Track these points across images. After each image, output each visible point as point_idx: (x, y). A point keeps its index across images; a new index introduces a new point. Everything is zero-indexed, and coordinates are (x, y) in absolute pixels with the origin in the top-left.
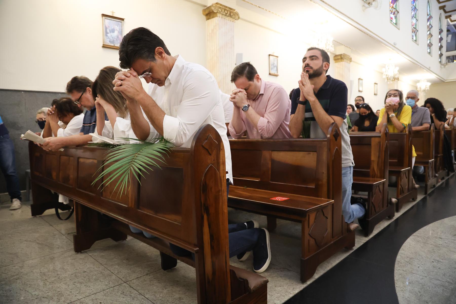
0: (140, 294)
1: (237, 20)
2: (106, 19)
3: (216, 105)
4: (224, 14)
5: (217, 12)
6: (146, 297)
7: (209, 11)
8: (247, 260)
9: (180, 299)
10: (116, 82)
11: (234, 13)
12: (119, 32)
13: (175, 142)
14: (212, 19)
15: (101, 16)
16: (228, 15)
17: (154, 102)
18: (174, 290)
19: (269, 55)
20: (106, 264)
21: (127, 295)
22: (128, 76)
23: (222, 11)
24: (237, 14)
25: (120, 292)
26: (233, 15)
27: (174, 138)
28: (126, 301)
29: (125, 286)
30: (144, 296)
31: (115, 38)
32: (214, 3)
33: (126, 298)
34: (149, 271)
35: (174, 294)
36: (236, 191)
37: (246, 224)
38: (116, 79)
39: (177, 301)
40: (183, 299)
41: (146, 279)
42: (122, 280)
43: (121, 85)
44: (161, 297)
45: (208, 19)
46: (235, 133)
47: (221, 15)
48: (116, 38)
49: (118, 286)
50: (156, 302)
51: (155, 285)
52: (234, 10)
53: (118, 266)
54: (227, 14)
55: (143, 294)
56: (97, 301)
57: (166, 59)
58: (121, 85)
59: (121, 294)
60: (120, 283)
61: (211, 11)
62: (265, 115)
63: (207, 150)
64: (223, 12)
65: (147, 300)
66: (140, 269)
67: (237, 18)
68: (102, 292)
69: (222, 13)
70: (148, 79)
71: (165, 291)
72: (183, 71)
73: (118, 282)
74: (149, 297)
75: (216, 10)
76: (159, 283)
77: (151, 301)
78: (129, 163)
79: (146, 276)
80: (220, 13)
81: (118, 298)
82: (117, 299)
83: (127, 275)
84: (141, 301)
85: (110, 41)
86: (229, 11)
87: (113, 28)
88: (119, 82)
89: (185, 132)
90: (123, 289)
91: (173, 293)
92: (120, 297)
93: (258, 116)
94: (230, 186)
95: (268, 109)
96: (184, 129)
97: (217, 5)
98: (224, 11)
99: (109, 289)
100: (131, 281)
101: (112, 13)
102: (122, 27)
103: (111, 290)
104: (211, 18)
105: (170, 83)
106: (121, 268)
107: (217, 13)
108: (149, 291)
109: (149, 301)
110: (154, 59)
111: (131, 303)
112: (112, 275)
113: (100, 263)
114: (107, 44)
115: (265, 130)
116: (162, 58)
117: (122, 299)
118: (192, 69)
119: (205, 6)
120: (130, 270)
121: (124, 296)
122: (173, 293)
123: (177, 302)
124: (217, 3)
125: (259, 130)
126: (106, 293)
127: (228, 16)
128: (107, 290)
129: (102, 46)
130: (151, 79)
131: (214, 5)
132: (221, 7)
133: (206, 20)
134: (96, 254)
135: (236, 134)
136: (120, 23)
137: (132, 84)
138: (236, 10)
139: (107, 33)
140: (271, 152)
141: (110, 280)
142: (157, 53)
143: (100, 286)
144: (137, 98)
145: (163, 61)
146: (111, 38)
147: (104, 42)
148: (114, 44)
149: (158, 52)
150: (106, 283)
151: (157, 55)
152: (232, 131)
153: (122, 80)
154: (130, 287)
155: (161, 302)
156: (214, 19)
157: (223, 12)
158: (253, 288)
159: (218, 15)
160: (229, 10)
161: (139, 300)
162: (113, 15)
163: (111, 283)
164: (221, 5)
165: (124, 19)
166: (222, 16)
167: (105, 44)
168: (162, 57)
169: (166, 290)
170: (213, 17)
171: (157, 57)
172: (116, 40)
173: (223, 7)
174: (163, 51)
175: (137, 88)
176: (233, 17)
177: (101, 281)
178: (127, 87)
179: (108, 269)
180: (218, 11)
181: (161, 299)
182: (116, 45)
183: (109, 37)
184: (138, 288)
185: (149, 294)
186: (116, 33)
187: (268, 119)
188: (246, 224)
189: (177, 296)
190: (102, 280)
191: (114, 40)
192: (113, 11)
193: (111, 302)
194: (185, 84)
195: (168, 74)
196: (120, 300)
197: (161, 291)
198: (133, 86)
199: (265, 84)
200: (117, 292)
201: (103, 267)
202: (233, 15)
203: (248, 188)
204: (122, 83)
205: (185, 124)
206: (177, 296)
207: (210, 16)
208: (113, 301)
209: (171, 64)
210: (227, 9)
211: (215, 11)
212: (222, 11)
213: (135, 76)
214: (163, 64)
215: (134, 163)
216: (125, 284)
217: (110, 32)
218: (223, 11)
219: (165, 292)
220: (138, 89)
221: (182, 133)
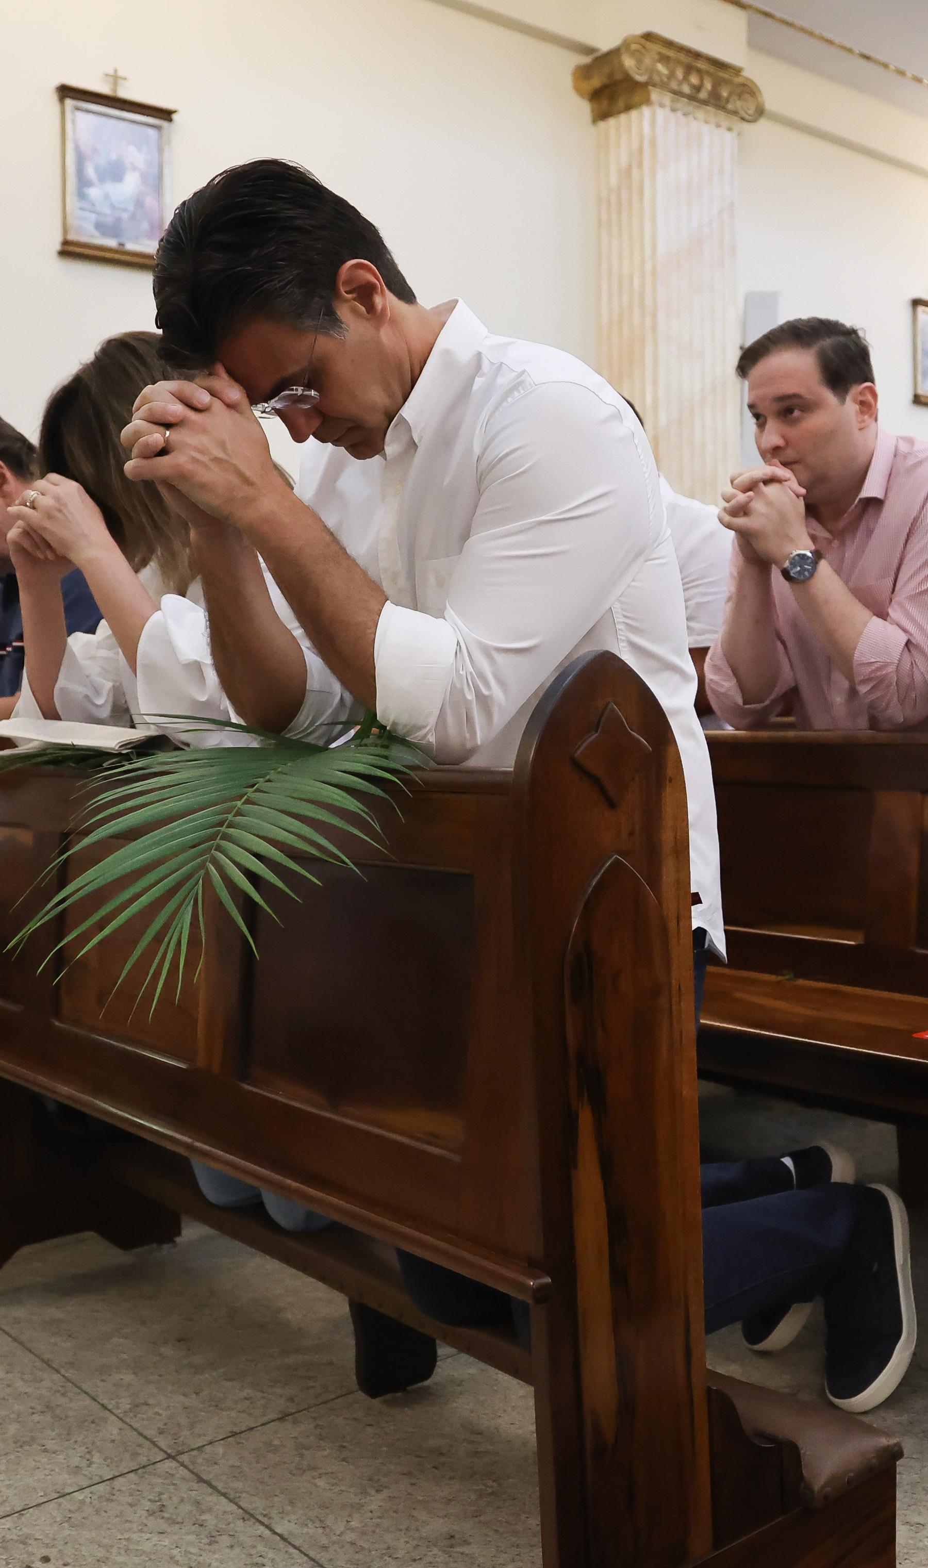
0: (249, 1515)
1: (748, 121)
2: (78, 109)
3: (641, 559)
4: (686, 89)
6: (275, 1533)
7: (611, 75)
8: (796, 1345)
9: (453, 1541)
10: (138, 435)
12: (144, 178)
13: (432, 739)
14: (623, 117)
15: (54, 98)
16: (703, 95)
17: (328, 538)
18: (421, 1498)
19: (916, 303)
20: (71, 1364)
21: (179, 1519)
22: (199, 406)
23: (672, 75)
24: (748, 90)
25: (147, 1505)
26: (731, 94)
27: (432, 720)
28: (175, 1552)
29: (173, 1475)
30: (268, 1527)
31: (125, 210)
32: (634, 36)
33: (176, 1537)
34: (291, 1400)
35: (422, 1515)
36: (738, 995)
37: (788, 1161)
38: (137, 423)
39: (435, 1551)
40: (469, 1544)
41: (276, 1442)
42: (153, 1443)
43: (163, 452)
44: (352, 1530)
45: (601, 115)
46: (740, 701)
47: (667, 98)
48: (131, 208)
49: (132, 1475)
50: (328, 1556)
51: (323, 1471)
52: (737, 71)
53: (134, 1373)
54: (698, 89)
55: (260, 1518)
56: (30, 1549)
57: (394, 322)
58: (163, 452)
59: (151, 1513)
60: (143, 1460)
61: (619, 76)
62: (894, 612)
63: (595, 780)
64: (680, 83)
65: (282, 1544)
66: (247, 1392)
67: (750, 112)
68: (52, 1505)
69: (674, 85)
70: (301, 421)
71: (376, 1501)
72: (479, 382)
73: (135, 1455)
74: (290, 1533)
76: (343, 1460)
77: (301, 1551)
78: (194, 846)
79: (277, 1423)
80: (663, 86)
81: (135, 1536)
82: (128, 1539)
83: (183, 1421)
84: (253, 1552)
85: (99, 226)
86: (708, 73)
87: (114, 156)
88: (157, 437)
89: (485, 692)
90: (157, 1489)
91: (415, 1513)
92: (145, 1529)
93: (860, 612)
94: (710, 969)
95: (912, 577)
96: (481, 676)
97: (649, 45)
98: (686, 78)
99: (87, 1491)
100: (199, 1449)
101: (111, 80)
102: (160, 150)
103: (100, 1497)
104: (619, 113)
105: (413, 445)
106: (149, 1382)
107: (650, 87)
108: (291, 1503)
109: (292, 1550)
110: (332, 319)
111: (201, 1559)
112: (105, 1420)
113: (43, 1360)
114: (84, 239)
115: (888, 687)
116: (369, 316)
117: (155, 1538)
118: (524, 372)
119: (587, 50)
120: (197, 1394)
121: (163, 1525)
122: (415, 1513)
123: (435, 1556)
124: (649, 36)
125: (863, 682)
126: (72, 1508)
127: (705, 103)
128: (79, 1496)
129: (58, 247)
130: (316, 423)
131: (634, 47)
134: (20, 1312)
135: (745, 703)
136: (152, 132)
137: (222, 445)
139: (83, 182)
140: (919, 796)
141: (93, 1443)
142: (347, 292)
143: (39, 1475)
144: (247, 515)
145: (378, 329)
146: (107, 210)
147: (65, 230)
148: (121, 241)
149: (354, 286)
150: (75, 1461)
151: (347, 301)
152: (723, 690)
153: (168, 426)
154: (198, 1482)
155: (357, 1557)
156: (634, 114)
157: (680, 83)
158: (823, 1487)
159: (655, 95)
160: (712, 69)
161: (242, 1545)
162: (115, 90)
163: (97, 1458)
164: (669, 44)
165: (175, 112)
166: (673, 101)
167: (72, 237)
168: (371, 308)
169: (385, 1493)
170: (628, 108)
171: (344, 312)
172: (133, 217)
173: (682, 57)
174: (380, 283)
175: (243, 468)
176: (730, 106)
177: (45, 1451)
178: (194, 460)
179: (84, 1386)
180: (656, 78)
181: (352, 1543)
182: (130, 246)
183: (93, 205)
184: (238, 1485)
185: (293, 1517)
186: (130, 185)
187: (905, 631)
188: (788, 1161)
189: (437, 1526)
190: (50, 1445)
191: (119, 220)
192: (116, 71)
193: (101, 1553)
194: (485, 449)
195: (399, 395)
196: (147, 1547)
197: (355, 1500)
198: (221, 455)
199: (892, 455)
200: (131, 1505)
201: (56, 1377)
203: (801, 982)
204: (167, 441)
205: (487, 651)
206: (437, 1526)
207: (612, 98)
208: (108, 1548)
209: (417, 346)
210: (700, 65)
212: (672, 75)
213: (231, 406)
214: (378, 343)
215: (225, 844)
216: (169, 1465)
217: (102, 179)
218: (680, 74)
219: (373, 1507)
220: (248, 473)
221: (470, 696)
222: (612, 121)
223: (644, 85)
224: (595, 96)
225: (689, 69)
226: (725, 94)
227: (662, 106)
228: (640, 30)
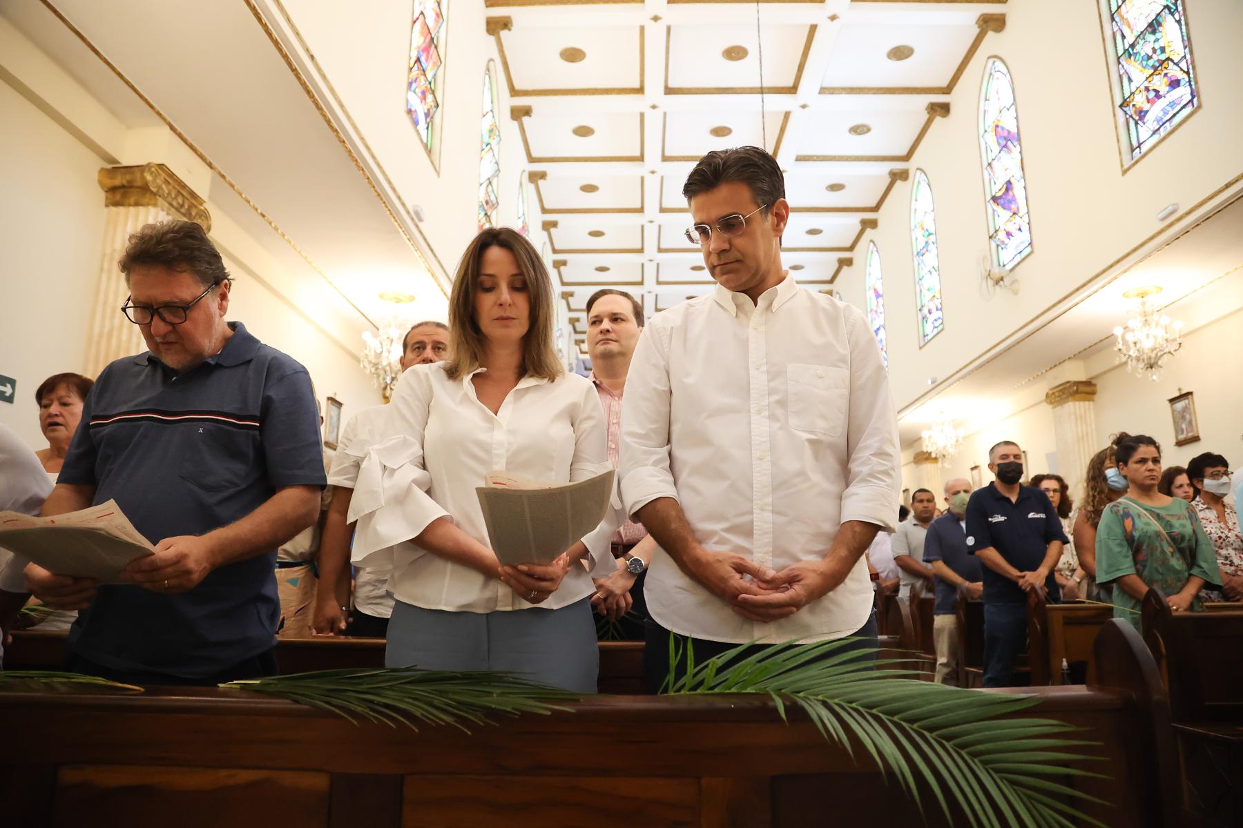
4: (175, 203)
5: (154, 194)
7: (129, 182)
11: (201, 210)
14: (132, 209)
16: (183, 210)
26: (196, 214)
54: (182, 206)
75: (156, 187)
80: (165, 198)
98: (176, 198)
104: (130, 205)
131: (153, 169)
133: (107, 206)
138: (205, 205)
156: (141, 209)
164: (172, 175)
170: (137, 204)
202: (195, 217)
207: (124, 195)
211: (154, 190)
212: (169, 194)
222: (121, 210)
223: (154, 194)
224: (112, 190)
226: (194, 214)
227: (163, 210)
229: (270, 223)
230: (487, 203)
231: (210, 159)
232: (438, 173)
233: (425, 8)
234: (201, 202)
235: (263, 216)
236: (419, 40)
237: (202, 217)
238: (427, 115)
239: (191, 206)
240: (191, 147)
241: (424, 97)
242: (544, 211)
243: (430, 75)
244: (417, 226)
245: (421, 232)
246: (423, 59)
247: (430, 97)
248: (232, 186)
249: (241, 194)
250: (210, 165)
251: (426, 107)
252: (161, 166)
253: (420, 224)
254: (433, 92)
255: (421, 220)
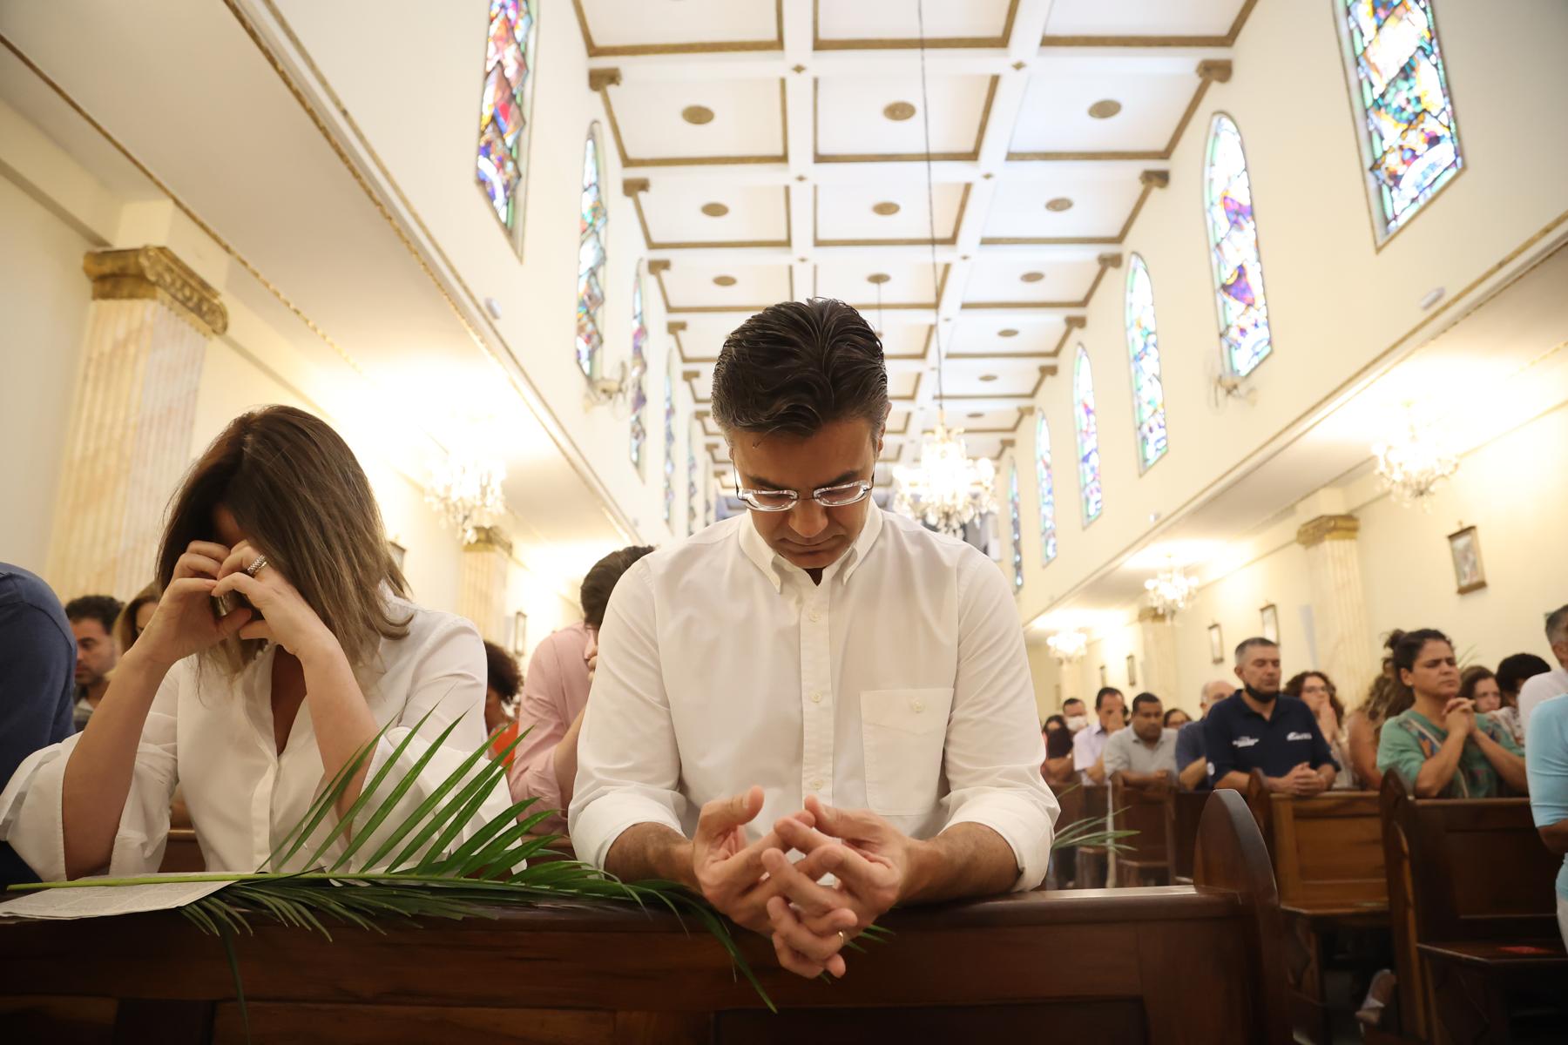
4: (180, 296)
5: (153, 284)
11: (213, 304)
14: (126, 303)
16: (191, 304)
26: (209, 309)
47: (168, 298)
54: (189, 299)
64: (178, 290)
80: (166, 288)
98: (182, 288)
104: (122, 297)
127: (192, 310)
132: (174, 267)
159: (160, 292)
160: (198, 287)
164: (176, 260)
170: (131, 296)
176: (207, 318)
210: (193, 283)
211: (152, 278)
212: (173, 283)
218: (178, 284)
223: (153, 284)
224: (100, 279)
225: (185, 284)
227: (163, 303)
228: (161, 242)
229: (307, 321)
230: (590, 297)
231: (226, 241)
232: (521, 259)
233: (504, 57)
234: (215, 294)
235: (297, 312)
236: (491, 95)
237: (218, 314)
238: (506, 187)
239: (202, 300)
240: (202, 225)
241: (501, 165)
242: (670, 309)
243: (509, 140)
244: (491, 324)
245: (496, 332)
246: (501, 120)
247: (510, 165)
248: (256, 275)
249: (267, 285)
250: (227, 249)
251: (505, 178)
252: (162, 250)
253: (496, 323)
254: (515, 162)
255: (495, 316)
